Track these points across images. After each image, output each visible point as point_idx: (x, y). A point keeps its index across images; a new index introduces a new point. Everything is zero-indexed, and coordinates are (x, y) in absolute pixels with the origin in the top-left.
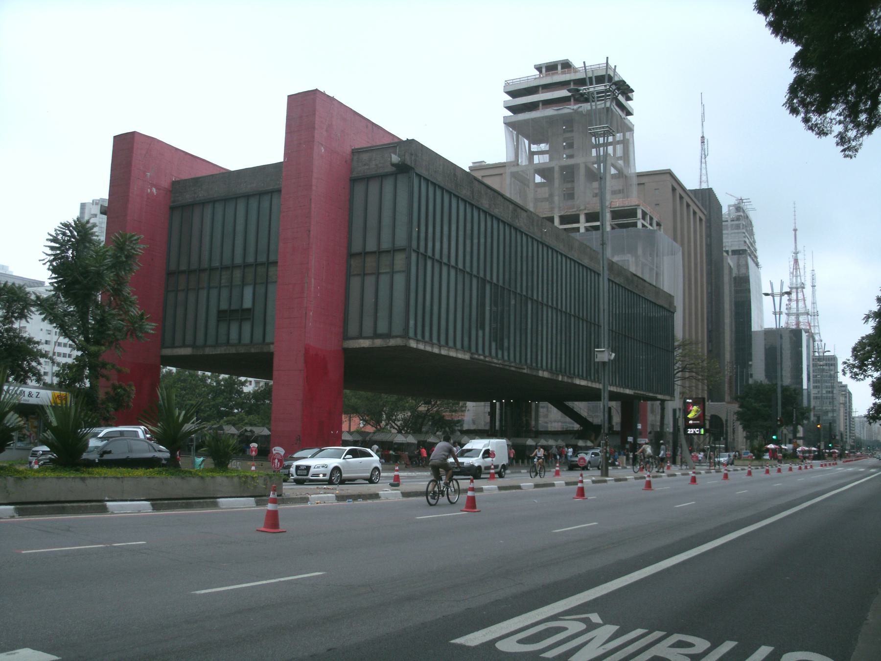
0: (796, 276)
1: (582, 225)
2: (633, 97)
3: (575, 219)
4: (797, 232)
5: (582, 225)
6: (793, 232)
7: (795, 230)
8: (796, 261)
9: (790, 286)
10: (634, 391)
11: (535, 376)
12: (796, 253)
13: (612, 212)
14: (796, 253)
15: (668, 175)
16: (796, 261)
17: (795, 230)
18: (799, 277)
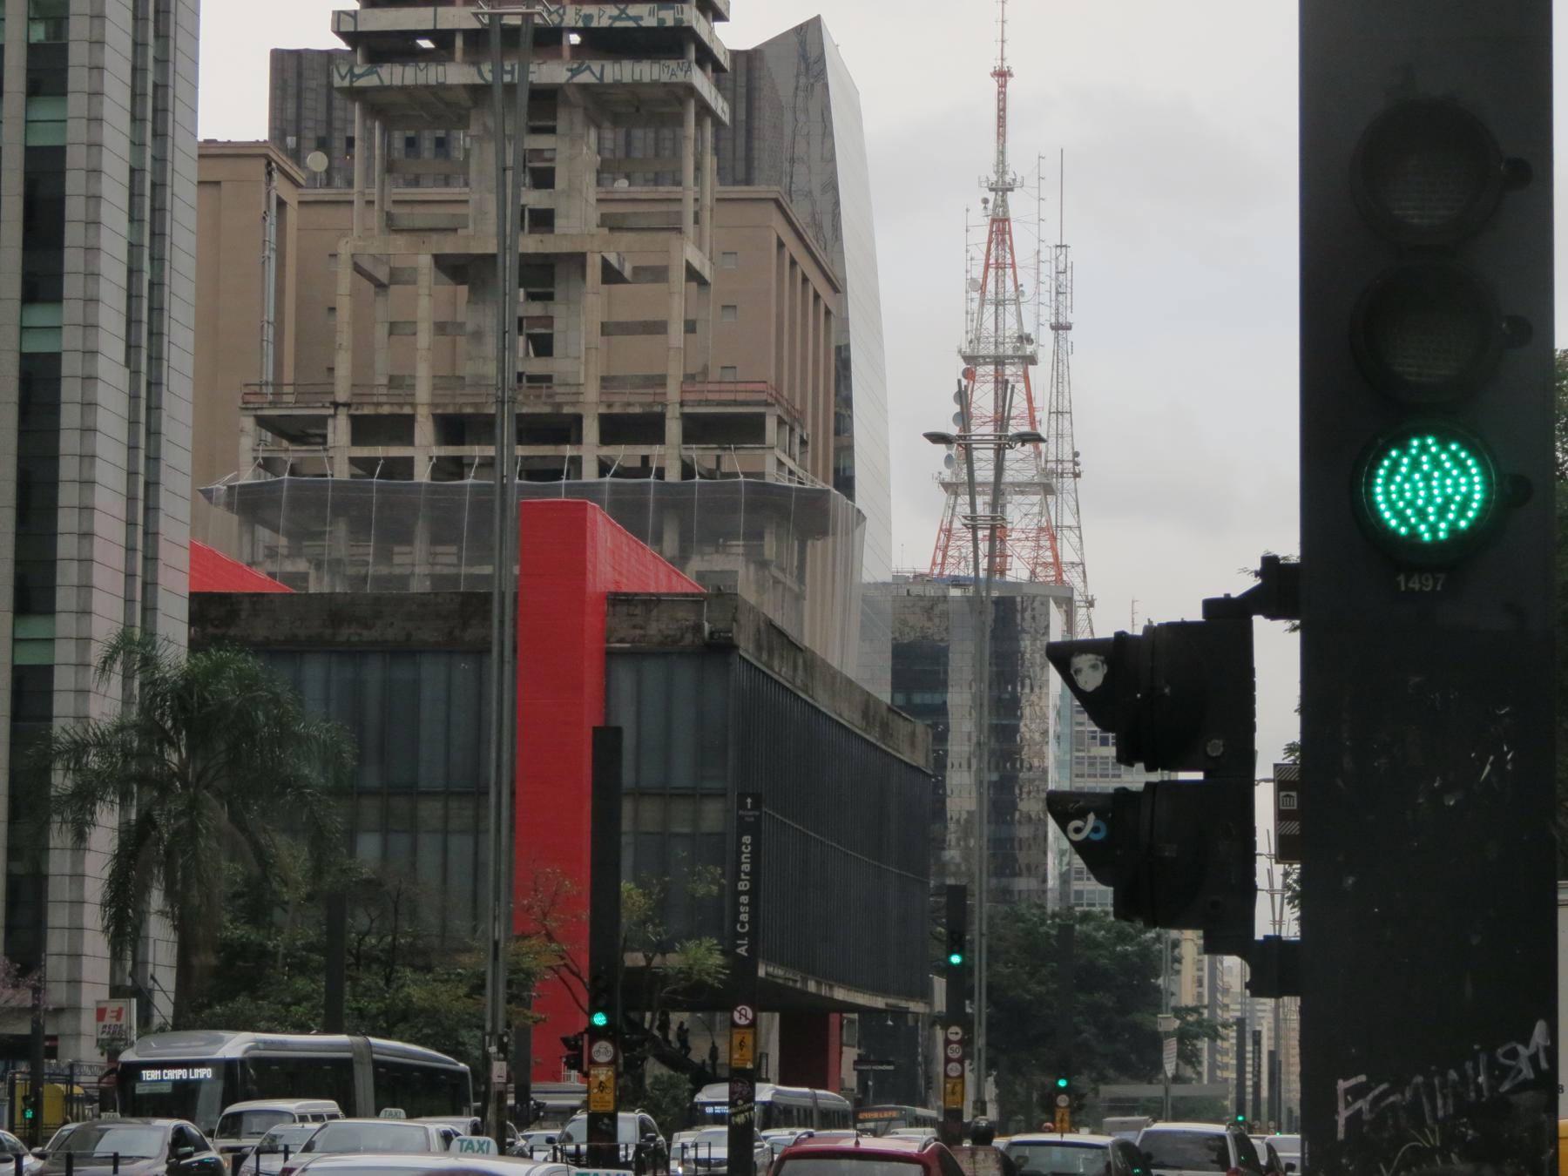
0: (999, 303)
1: (590, 449)
2: (728, 9)
3: (565, 429)
4: (1011, 83)
5: (590, 449)
6: (993, 84)
7: (1002, 75)
8: (1000, 226)
9: (968, 351)
10: (885, 1000)
11: (825, 998)
12: (1002, 189)
13: (686, 417)
14: (1002, 189)
15: (772, 207)
16: (1000, 226)
17: (1002, 75)
18: (1011, 308)
